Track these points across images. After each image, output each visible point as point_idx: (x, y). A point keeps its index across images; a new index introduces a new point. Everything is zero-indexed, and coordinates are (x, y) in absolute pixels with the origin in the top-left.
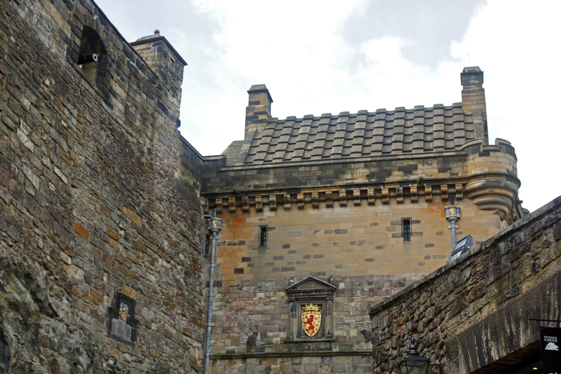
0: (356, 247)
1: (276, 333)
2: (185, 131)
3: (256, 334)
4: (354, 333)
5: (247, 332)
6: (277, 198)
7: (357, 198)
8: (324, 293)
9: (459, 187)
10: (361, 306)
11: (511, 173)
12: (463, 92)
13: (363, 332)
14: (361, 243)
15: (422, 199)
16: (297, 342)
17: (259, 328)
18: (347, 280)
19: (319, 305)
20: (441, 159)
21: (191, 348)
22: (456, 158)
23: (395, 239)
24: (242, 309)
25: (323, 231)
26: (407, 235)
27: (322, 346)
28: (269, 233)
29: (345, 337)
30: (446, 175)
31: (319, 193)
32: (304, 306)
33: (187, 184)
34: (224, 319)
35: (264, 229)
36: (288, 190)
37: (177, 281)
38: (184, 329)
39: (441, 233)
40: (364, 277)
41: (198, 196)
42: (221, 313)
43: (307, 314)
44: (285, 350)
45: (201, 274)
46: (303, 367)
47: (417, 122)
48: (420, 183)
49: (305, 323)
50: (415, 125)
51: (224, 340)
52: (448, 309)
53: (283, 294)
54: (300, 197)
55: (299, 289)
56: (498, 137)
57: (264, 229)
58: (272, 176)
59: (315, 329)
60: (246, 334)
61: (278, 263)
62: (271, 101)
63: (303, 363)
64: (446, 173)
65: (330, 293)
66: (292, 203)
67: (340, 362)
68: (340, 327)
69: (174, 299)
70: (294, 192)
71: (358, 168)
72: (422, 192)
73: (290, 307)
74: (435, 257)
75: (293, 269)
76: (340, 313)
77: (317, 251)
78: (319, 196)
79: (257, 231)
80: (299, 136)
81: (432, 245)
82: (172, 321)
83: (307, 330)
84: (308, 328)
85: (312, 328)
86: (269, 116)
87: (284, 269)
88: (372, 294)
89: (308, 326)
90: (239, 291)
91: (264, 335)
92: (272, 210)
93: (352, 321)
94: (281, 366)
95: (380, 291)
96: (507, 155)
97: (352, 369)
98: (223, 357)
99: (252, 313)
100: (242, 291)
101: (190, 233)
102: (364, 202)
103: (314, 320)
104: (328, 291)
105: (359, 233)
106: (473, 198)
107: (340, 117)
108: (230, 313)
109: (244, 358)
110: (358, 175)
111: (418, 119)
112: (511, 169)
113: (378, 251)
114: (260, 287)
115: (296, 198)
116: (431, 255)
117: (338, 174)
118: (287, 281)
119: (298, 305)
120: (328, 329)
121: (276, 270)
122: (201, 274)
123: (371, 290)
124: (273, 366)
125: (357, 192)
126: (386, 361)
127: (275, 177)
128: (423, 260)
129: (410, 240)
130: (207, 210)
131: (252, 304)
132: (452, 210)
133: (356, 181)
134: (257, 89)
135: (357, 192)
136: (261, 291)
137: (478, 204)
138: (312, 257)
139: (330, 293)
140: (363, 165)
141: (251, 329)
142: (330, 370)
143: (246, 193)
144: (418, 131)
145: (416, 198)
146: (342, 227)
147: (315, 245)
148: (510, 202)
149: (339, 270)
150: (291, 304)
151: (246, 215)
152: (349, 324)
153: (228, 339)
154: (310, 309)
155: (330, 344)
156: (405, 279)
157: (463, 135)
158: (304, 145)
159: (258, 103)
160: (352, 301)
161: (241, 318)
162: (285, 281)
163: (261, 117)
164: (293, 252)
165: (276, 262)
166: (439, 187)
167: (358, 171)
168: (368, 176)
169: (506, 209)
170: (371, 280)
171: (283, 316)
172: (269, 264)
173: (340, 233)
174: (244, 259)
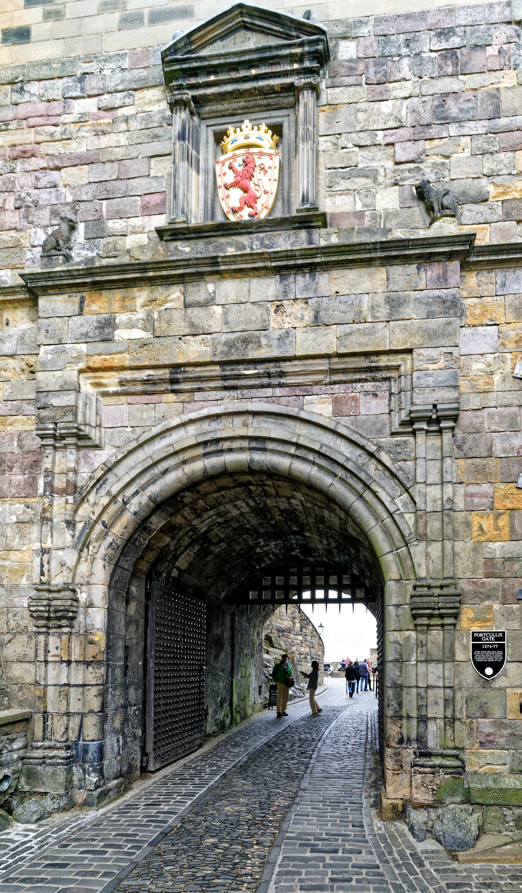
4: (388, 200)
43: (234, 157)
49: (227, 187)
84: (237, 205)
93: (382, 162)
94: (149, 314)
103: (258, 174)
152: (371, 174)
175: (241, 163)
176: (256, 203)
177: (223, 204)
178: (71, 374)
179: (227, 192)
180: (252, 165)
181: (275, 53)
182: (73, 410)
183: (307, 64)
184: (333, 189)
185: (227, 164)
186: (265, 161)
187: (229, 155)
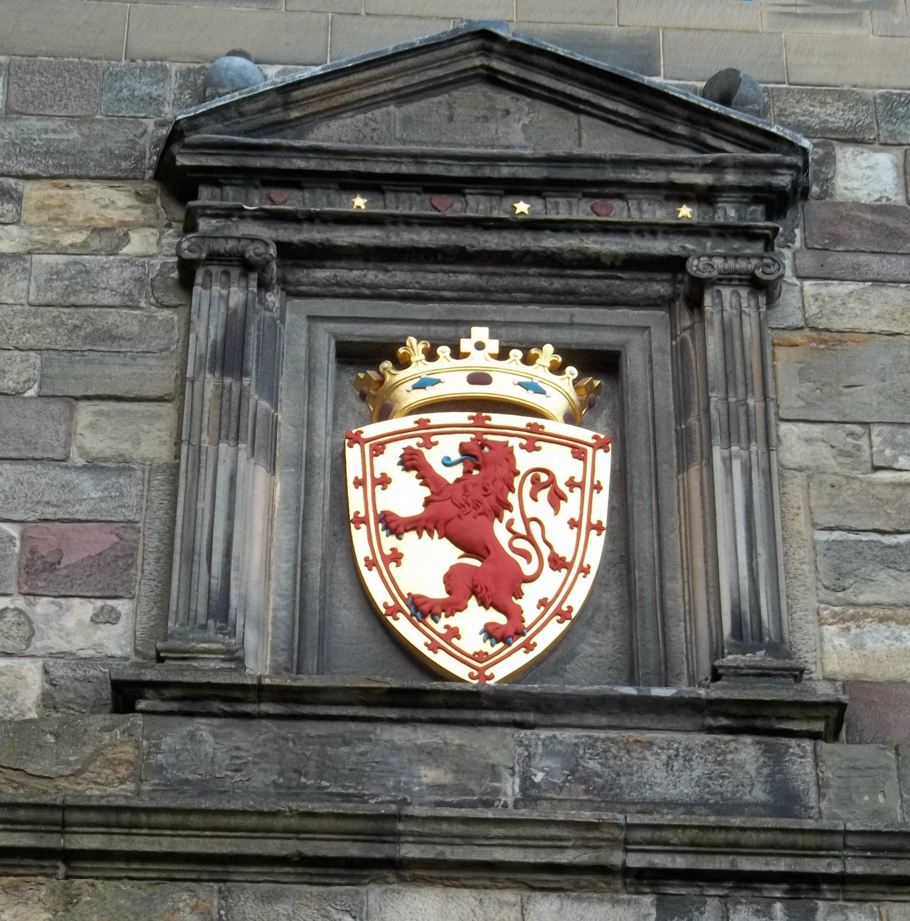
8: (658, 213)
16: (291, 701)
27: (672, 770)
49: (393, 525)
55: (330, 134)
73: (208, 329)
84: (438, 592)
85: (490, 580)
89: (428, 564)
104: (704, 197)
118: (170, 89)
150: (219, 299)
155: (776, 758)
162: (143, 88)
171: (95, 432)
175: (456, 456)
176: (519, 595)
177: (372, 579)
179: (389, 542)
180: (503, 471)
181: (611, 174)
183: (728, 212)
184: (849, 595)
185: (394, 451)
186: (559, 462)
187: (409, 422)
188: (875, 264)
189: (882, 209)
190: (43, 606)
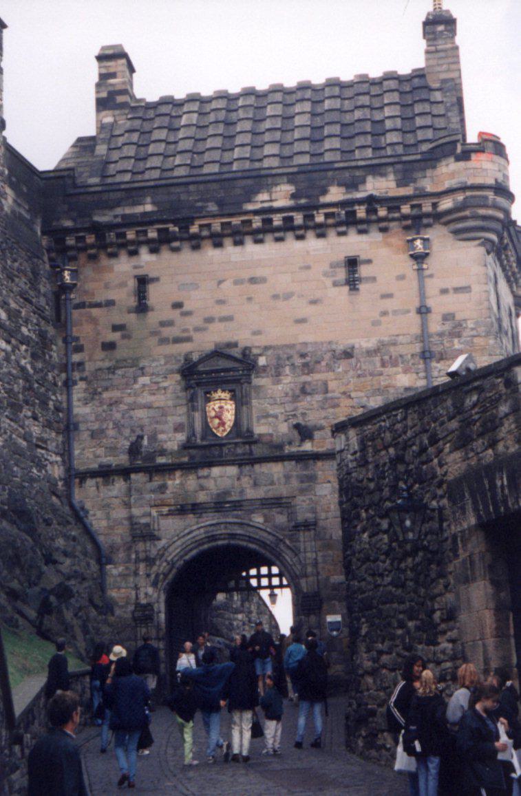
0: (280, 304)
1: (170, 435)
2: (13, 136)
3: (141, 437)
4: (284, 428)
5: (127, 435)
6: (159, 235)
7: (278, 229)
9: (427, 208)
10: (292, 390)
11: (500, 184)
12: (427, 52)
13: (297, 427)
14: (288, 296)
15: (374, 228)
17: (146, 429)
18: (270, 352)
19: (230, 391)
20: (399, 167)
21: (49, 465)
22: (423, 164)
23: (337, 289)
24: (117, 402)
25: (232, 280)
26: (352, 283)
28: (152, 290)
29: (271, 435)
30: (407, 191)
31: (222, 224)
32: (209, 393)
33: (20, 217)
34: (93, 418)
35: (143, 282)
36: (175, 222)
37: (23, 369)
38: (38, 439)
39: (402, 278)
40: (292, 346)
41: (39, 233)
42: (87, 410)
44: (186, 459)
45: (52, 353)
46: (212, 481)
47: (359, 103)
48: (370, 204)
50: (356, 107)
51: (94, 449)
52: (449, 438)
53: (178, 377)
54: (194, 229)
55: (201, 368)
56: (482, 131)
57: (143, 282)
58: (149, 199)
59: (226, 426)
60: (126, 438)
61: (167, 332)
62: (132, 69)
63: (213, 475)
64: (407, 188)
65: (245, 372)
66: (182, 239)
67: (266, 472)
68: (263, 421)
69: (21, 396)
70: (185, 223)
71: (279, 184)
72: (374, 217)
74: (395, 312)
75: (189, 339)
76: (262, 401)
77: (225, 311)
78: (222, 229)
79: (132, 284)
80: (182, 130)
81: (389, 296)
82: (20, 429)
83: (216, 429)
85: (223, 424)
86: (132, 97)
87: (177, 340)
88: (306, 371)
89: (217, 421)
90: (111, 376)
91: (153, 438)
92: (154, 251)
95: (318, 366)
96: (496, 158)
97: (283, 480)
98: (93, 474)
99: (133, 407)
100: (116, 376)
101: (32, 293)
102: (290, 236)
105: (283, 282)
106: (446, 224)
107: (242, 95)
108: (100, 409)
109: (125, 473)
110: (278, 194)
111: (361, 97)
112: (500, 179)
113: (313, 307)
114: (142, 369)
115: (188, 232)
116: (390, 311)
117: (249, 195)
119: (200, 392)
120: (245, 422)
121: (164, 341)
122: (52, 353)
123: (306, 365)
124: (170, 483)
125: (277, 220)
126: (359, 496)
127: (153, 203)
128: (378, 317)
129: (358, 289)
130: (53, 255)
131: (132, 394)
132: (418, 243)
133: (276, 204)
134: (110, 52)
135: (277, 220)
136: (143, 375)
137: (456, 232)
138: (217, 320)
139: (245, 372)
140: (285, 179)
141: (133, 431)
142: (251, 482)
143: (111, 227)
144: (361, 118)
145: (364, 227)
146: (259, 273)
147: (221, 302)
148: (498, 226)
149: (258, 337)
151: (113, 261)
152: (276, 417)
153: (101, 447)
154: (217, 398)
156: (353, 348)
157: (429, 123)
158: (192, 145)
159: (113, 75)
160: (279, 382)
161: (118, 416)
163: (120, 99)
164: (188, 314)
165: (163, 329)
166: (398, 209)
167: (278, 188)
168: (293, 196)
169: (494, 237)
170: (304, 351)
172: (154, 333)
173: (255, 283)
174: (116, 328)
178: (147, 509)
182: (148, 525)
188: (263, 375)
189: (264, 366)
190: (176, 435)
